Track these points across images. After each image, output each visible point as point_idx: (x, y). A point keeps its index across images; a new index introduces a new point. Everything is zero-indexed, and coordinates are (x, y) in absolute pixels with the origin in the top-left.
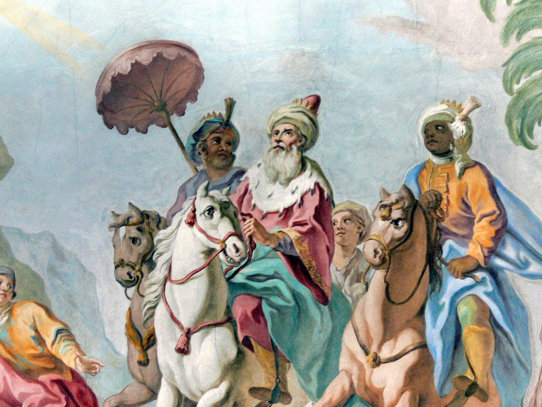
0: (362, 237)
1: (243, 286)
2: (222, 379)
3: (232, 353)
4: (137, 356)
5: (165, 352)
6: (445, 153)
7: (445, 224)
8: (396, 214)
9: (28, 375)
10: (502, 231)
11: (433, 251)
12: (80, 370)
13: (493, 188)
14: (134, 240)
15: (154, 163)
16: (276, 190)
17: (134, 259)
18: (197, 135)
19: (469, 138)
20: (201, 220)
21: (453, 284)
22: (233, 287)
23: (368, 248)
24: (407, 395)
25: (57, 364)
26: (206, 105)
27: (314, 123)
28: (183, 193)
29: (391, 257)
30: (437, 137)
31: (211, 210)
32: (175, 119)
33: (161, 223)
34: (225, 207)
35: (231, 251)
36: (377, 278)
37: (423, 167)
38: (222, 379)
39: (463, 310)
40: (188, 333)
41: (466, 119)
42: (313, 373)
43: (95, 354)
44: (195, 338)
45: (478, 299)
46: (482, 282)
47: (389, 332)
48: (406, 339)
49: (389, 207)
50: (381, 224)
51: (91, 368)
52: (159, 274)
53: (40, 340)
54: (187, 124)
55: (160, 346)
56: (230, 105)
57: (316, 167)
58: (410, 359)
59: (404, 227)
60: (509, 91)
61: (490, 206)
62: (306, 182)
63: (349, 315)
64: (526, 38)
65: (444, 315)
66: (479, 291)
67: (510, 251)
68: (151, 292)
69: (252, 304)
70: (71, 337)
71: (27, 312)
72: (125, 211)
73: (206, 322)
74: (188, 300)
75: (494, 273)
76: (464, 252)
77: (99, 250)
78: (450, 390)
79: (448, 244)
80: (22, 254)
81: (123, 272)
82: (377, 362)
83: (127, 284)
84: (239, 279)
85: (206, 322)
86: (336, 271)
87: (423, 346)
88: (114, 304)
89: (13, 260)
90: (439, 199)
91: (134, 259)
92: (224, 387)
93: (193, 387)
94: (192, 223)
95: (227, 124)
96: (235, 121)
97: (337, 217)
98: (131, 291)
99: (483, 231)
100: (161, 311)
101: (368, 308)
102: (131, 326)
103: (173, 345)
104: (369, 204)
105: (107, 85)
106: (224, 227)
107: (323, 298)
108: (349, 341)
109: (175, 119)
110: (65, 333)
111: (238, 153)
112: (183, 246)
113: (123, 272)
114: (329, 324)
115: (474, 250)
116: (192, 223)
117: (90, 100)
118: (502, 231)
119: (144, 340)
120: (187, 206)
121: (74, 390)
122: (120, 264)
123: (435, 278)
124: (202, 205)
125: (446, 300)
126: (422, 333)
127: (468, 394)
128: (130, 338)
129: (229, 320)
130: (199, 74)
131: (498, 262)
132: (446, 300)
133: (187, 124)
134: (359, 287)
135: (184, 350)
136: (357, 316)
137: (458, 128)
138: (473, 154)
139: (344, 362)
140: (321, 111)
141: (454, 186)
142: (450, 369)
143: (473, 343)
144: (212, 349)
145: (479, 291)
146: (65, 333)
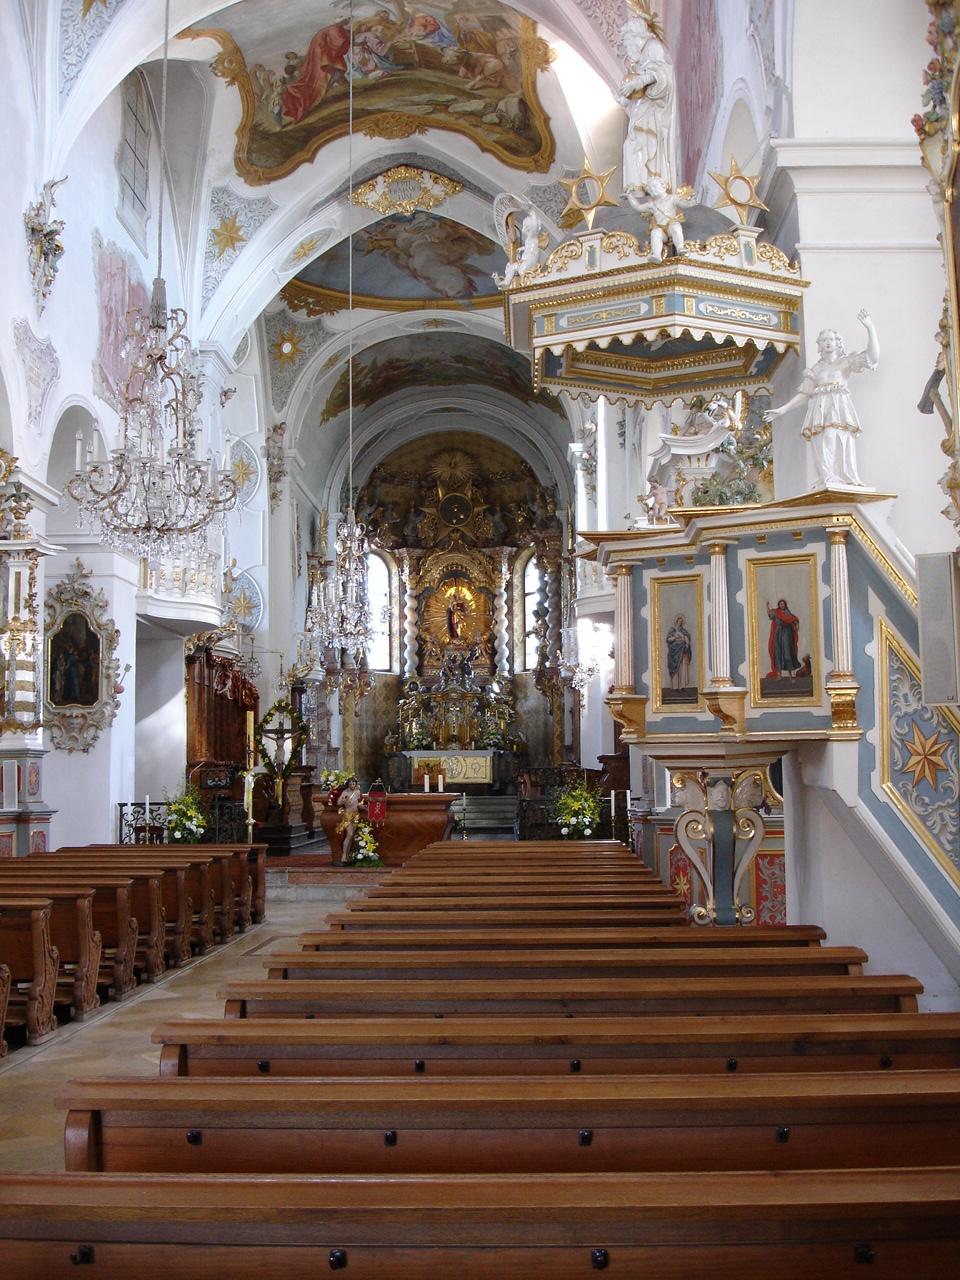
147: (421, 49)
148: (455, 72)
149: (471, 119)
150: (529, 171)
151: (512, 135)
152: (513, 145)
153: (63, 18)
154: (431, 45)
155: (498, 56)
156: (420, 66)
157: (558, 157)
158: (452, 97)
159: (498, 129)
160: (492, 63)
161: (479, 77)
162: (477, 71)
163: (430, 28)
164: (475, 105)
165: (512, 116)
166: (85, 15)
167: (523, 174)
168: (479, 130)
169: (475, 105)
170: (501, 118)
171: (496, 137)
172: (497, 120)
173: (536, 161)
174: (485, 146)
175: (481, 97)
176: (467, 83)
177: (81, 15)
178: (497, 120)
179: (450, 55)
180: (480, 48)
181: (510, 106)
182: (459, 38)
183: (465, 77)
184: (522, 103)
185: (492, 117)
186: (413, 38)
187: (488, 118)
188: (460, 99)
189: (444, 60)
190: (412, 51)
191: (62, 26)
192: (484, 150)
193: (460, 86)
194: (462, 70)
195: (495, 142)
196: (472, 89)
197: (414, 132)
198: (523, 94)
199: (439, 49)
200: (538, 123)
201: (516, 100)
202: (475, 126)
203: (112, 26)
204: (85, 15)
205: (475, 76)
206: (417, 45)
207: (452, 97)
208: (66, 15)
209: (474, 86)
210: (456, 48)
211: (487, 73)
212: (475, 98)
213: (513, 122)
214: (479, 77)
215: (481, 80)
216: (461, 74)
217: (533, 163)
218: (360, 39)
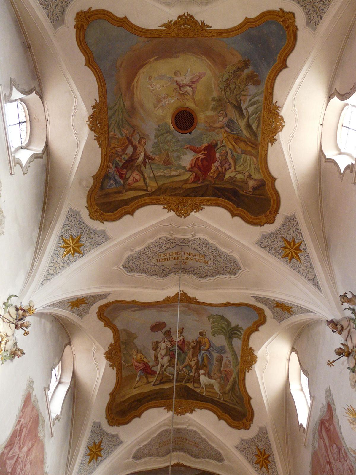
0: (189, 345)
1: (171, 350)
2: (168, 362)
3: (170, 359)
4: (156, 359)
5: (160, 359)
6: (202, 336)
7: (202, 344)
8: (195, 342)
9: (139, 363)
10: (210, 346)
11: (200, 347)
12: (147, 362)
13: (209, 341)
14: (155, 345)
15: (159, 336)
16: (177, 339)
17: (155, 347)
18: (165, 332)
19: (206, 334)
20: (165, 342)
21: (203, 352)
22: (170, 351)
23: (190, 346)
24: (195, 366)
25: (144, 361)
26: (167, 328)
27: (183, 331)
28: (163, 339)
29: (194, 348)
30: (201, 334)
31: (167, 341)
32: (162, 330)
33: (160, 343)
34: (169, 341)
35: (170, 346)
36: (192, 350)
37: (199, 337)
38: (168, 362)
39: (204, 355)
40: (163, 357)
41: (205, 332)
42: (182, 362)
43: (149, 360)
44: (164, 357)
45: (206, 354)
46: (207, 352)
47: (193, 357)
48: (195, 358)
49: (194, 342)
50: (192, 343)
51: (149, 362)
52: (159, 349)
53: (141, 358)
54: (164, 331)
55: (159, 358)
56: (170, 329)
57: (183, 336)
58: (196, 361)
59: (196, 344)
60: (212, 330)
61: (209, 343)
62: (181, 338)
63: (187, 355)
64: (214, 324)
65: (201, 356)
66: (207, 353)
67: (211, 349)
68: (158, 351)
69: (173, 353)
70: (146, 358)
71: (139, 355)
72: (154, 341)
73: (166, 355)
74: (163, 352)
75: (209, 351)
76: (204, 348)
77: (150, 346)
78: (202, 366)
79: (202, 347)
80: (139, 347)
81: (154, 349)
82: (191, 361)
83: (154, 350)
84: (171, 349)
85: (166, 355)
86: (185, 349)
87: (198, 360)
88: (152, 353)
89: (137, 348)
90: (201, 342)
91: (155, 347)
92: (168, 363)
93: (164, 363)
94: (164, 342)
95: (170, 331)
96: (171, 330)
97: (186, 342)
98: (155, 351)
99: (207, 346)
100: (159, 354)
101: (190, 354)
102: (155, 356)
103: (161, 358)
104: (191, 341)
105: (152, 327)
106: (169, 343)
107: (183, 352)
108: (187, 358)
109: (162, 330)
110: (145, 357)
111: (171, 334)
112: (163, 345)
113: (154, 349)
114: (184, 355)
115: (206, 348)
116: (164, 342)
117: (149, 328)
118: (210, 346)
119: (156, 357)
120: (163, 341)
121: (146, 364)
122: (153, 348)
123: (200, 351)
124: (166, 340)
125: (202, 354)
126: (198, 358)
127: (204, 366)
128: (155, 358)
129: (169, 355)
130: (166, 325)
131: (210, 350)
132: (202, 354)
133: (164, 331)
134: (189, 351)
135: (162, 359)
136: (188, 355)
137: (204, 333)
138: (206, 336)
139: (186, 361)
140: (184, 329)
141: (203, 340)
142: (202, 363)
143: (205, 360)
144: (166, 359)
145: (207, 353)
146: (145, 357)
153: (81, 463)
166: (89, 464)
177: (87, 463)
191: (80, 466)
203: (97, 469)
204: (89, 464)
208: (82, 463)
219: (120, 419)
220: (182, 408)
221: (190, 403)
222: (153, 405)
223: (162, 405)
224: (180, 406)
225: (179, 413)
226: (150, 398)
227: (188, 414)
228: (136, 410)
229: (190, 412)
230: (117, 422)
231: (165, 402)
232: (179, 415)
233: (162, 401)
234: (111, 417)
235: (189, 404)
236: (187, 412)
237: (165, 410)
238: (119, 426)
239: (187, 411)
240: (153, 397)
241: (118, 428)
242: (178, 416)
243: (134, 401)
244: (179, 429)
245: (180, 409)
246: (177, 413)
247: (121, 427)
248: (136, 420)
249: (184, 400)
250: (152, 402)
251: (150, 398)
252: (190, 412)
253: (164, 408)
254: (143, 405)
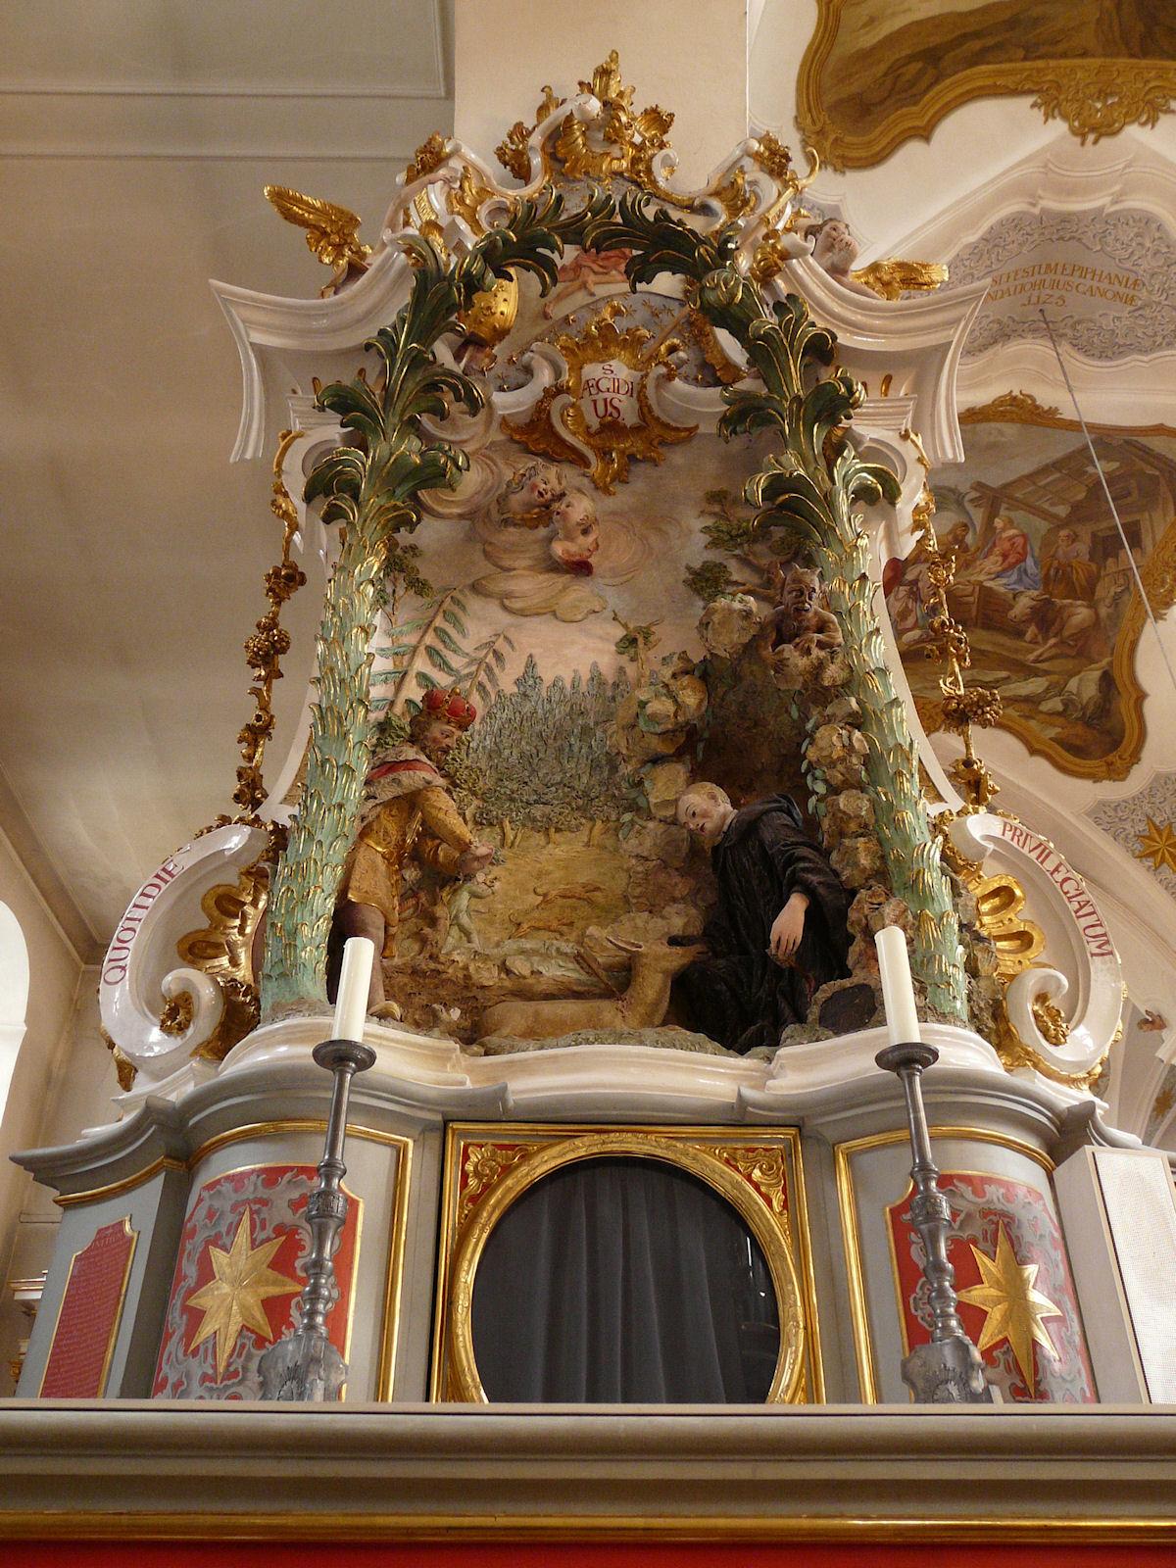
147: (986, 594)
148: (1019, 634)
149: (1023, 706)
150: (1096, 778)
151: (1079, 729)
152: (1078, 742)
154: (1002, 590)
155: (1093, 605)
156: (975, 625)
157: (1147, 753)
158: (1004, 674)
159: (1061, 720)
160: (1081, 614)
161: (1052, 641)
162: (1054, 629)
163: (1011, 559)
164: (1034, 686)
165: (1084, 702)
167: (1087, 784)
168: (1032, 723)
169: (1034, 686)
170: (1066, 704)
171: (1053, 732)
172: (1060, 708)
173: (1110, 764)
174: (1037, 746)
175: (1046, 673)
176: (1032, 651)
178: (1060, 708)
179: (1023, 605)
180: (1072, 593)
181: (1085, 686)
182: (1047, 575)
183: (1034, 642)
184: (1107, 681)
185: (1055, 704)
186: (982, 578)
187: (1045, 707)
188: (1014, 678)
189: (1012, 614)
190: (971, 599)
192: (1033, 751)
193: (1020, 657)
194: (1031, 631)
195: (1050, 739)
196: (1036, 661)
197: (937, 730)
198: (1111, 664)
199: (1011, 596)
200: (1124, 706)
201: (1097, 674)
202: (1028, 718)
205: (1046, 639)
206: (982, 588)
207: (1004, 674)
209: (1040, 655)
210: (1036, 593)
211: (1066, 633)
212: (1036, 676)
213: (1084, 708)
214: (1052, 641)
215: (1055, 645)
216: (1028, 636)
217: (1104, 769)
218: (910, 577)
219: (848, 139)
220: (1110, 102)
221: (1153, 74)
222: (989, 82)
223: (1026, 87)
224: (1100, 92)
225: (1093, 129)
226: (976, 45)
227: (1134, 132)
228: (915, 104)
229: (1144, 118)
230: (839, 152)
231: (1039, 71)
232: (1091, 137)
233: (1028, 64)
234: (814, 122)
235: (1147, 82)
236: (1133, 122)
237: (1036, 110)
238: (843, 173)
239: (1131, 116)
240: (990, 41)
241: (839, 178)
242: (1083, 144)
243: (912, 58)
244: (1065, 218)
245: (1099, 105)
246: (1082, 126)
247: (853, 177)
248: (913, 149)
249: (1123, 61)
250: (983, 68)
251: (976, 45)
252: (1144, 118)
253: (1030, 100)
254: (948, 81)
